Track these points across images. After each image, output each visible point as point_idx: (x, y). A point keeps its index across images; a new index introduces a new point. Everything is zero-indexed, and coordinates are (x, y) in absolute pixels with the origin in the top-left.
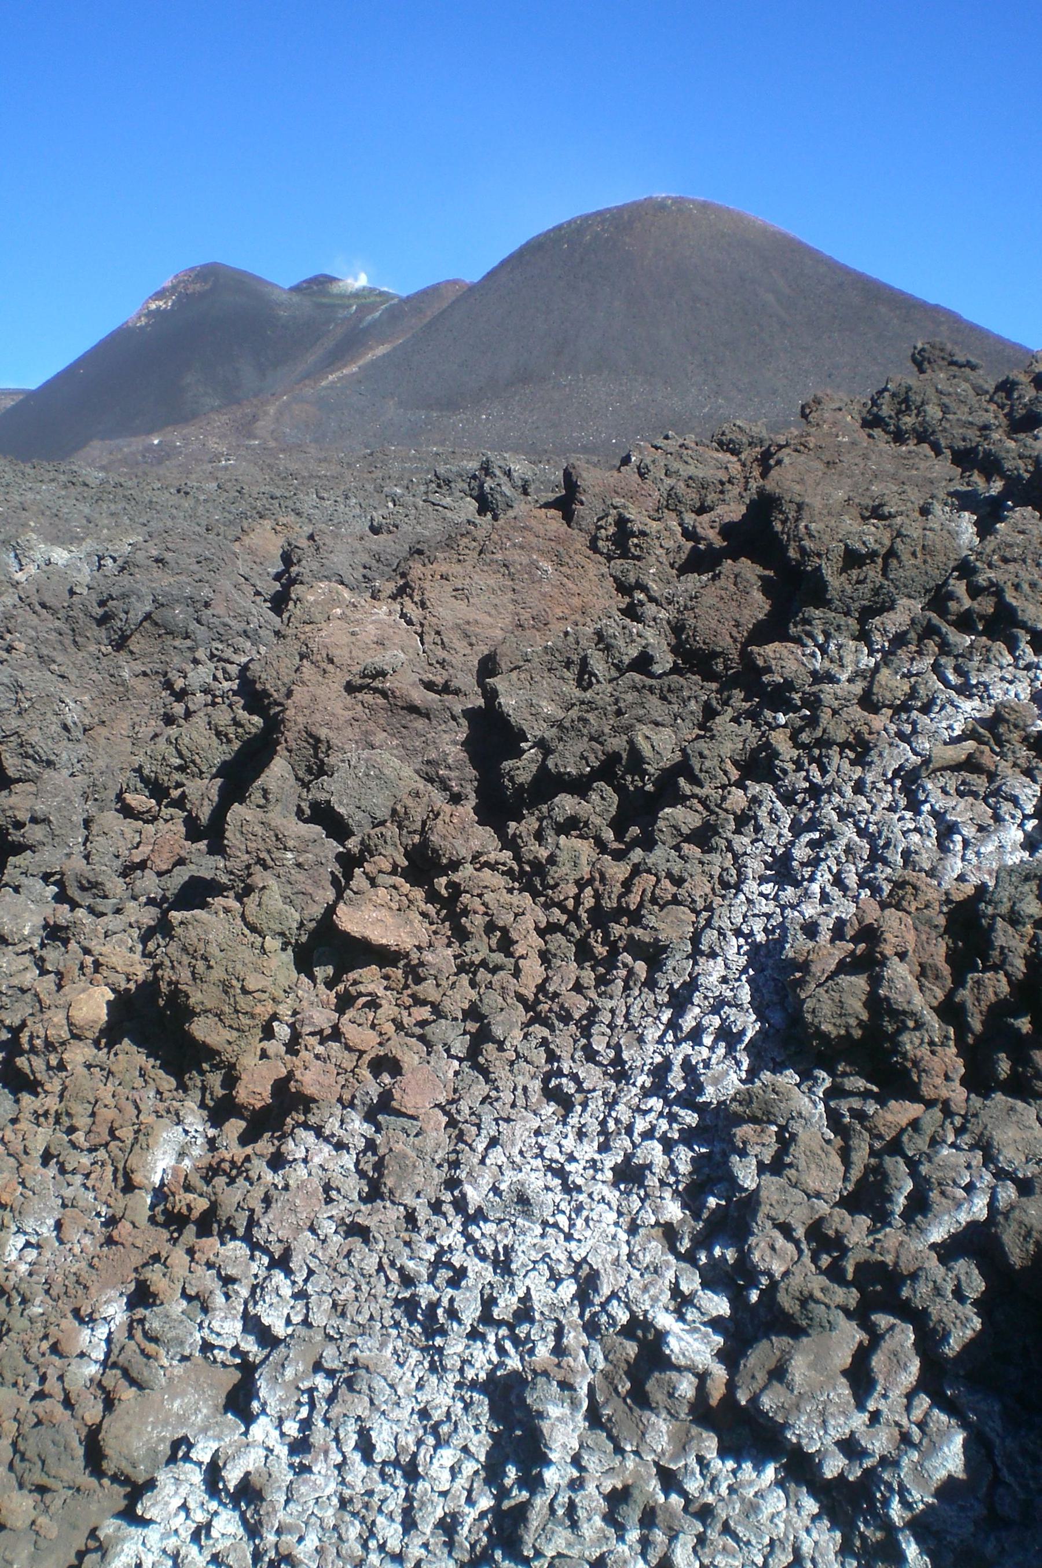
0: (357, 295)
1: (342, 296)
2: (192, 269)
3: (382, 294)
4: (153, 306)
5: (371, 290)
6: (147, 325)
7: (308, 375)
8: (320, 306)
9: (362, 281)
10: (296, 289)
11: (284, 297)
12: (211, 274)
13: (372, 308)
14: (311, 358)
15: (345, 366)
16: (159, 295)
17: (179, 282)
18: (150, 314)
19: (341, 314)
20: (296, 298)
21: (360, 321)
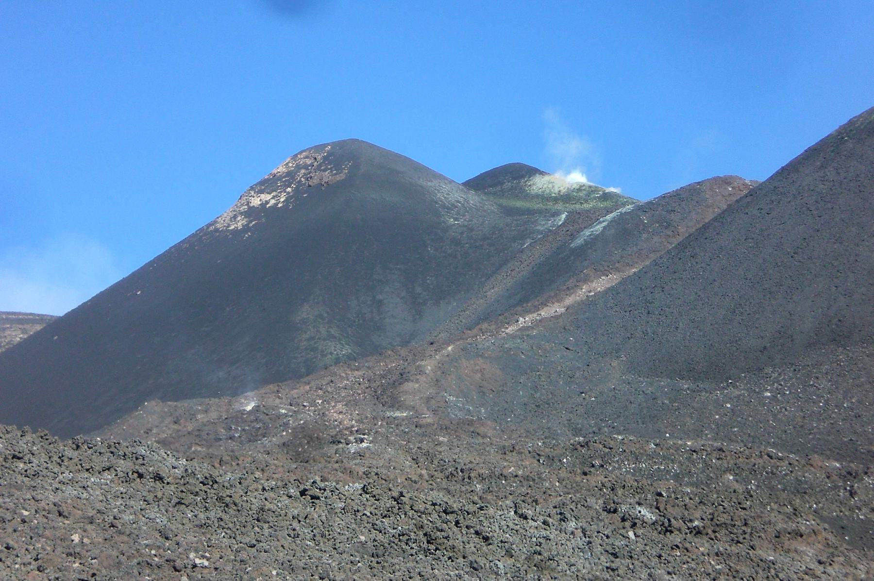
0: (567, 197)
1: (545, 198)
2: (319, 148)
3: (606, 196)
4: (256, 202)
5: (592, 190)
6: (246, 228)
7: (486, 317)
8: (509, 212)
9: (577, 178)
10: (477, 184)
11: (457, 196)
12: (344, 155)
13: (591, 217)
14: (495, 289)
15: (544, 304)
16: (267, 185)
17: (298, 167)
18: (251, 213)
19: (544, 225)
20: (473, 198)
21: (573, 237)
